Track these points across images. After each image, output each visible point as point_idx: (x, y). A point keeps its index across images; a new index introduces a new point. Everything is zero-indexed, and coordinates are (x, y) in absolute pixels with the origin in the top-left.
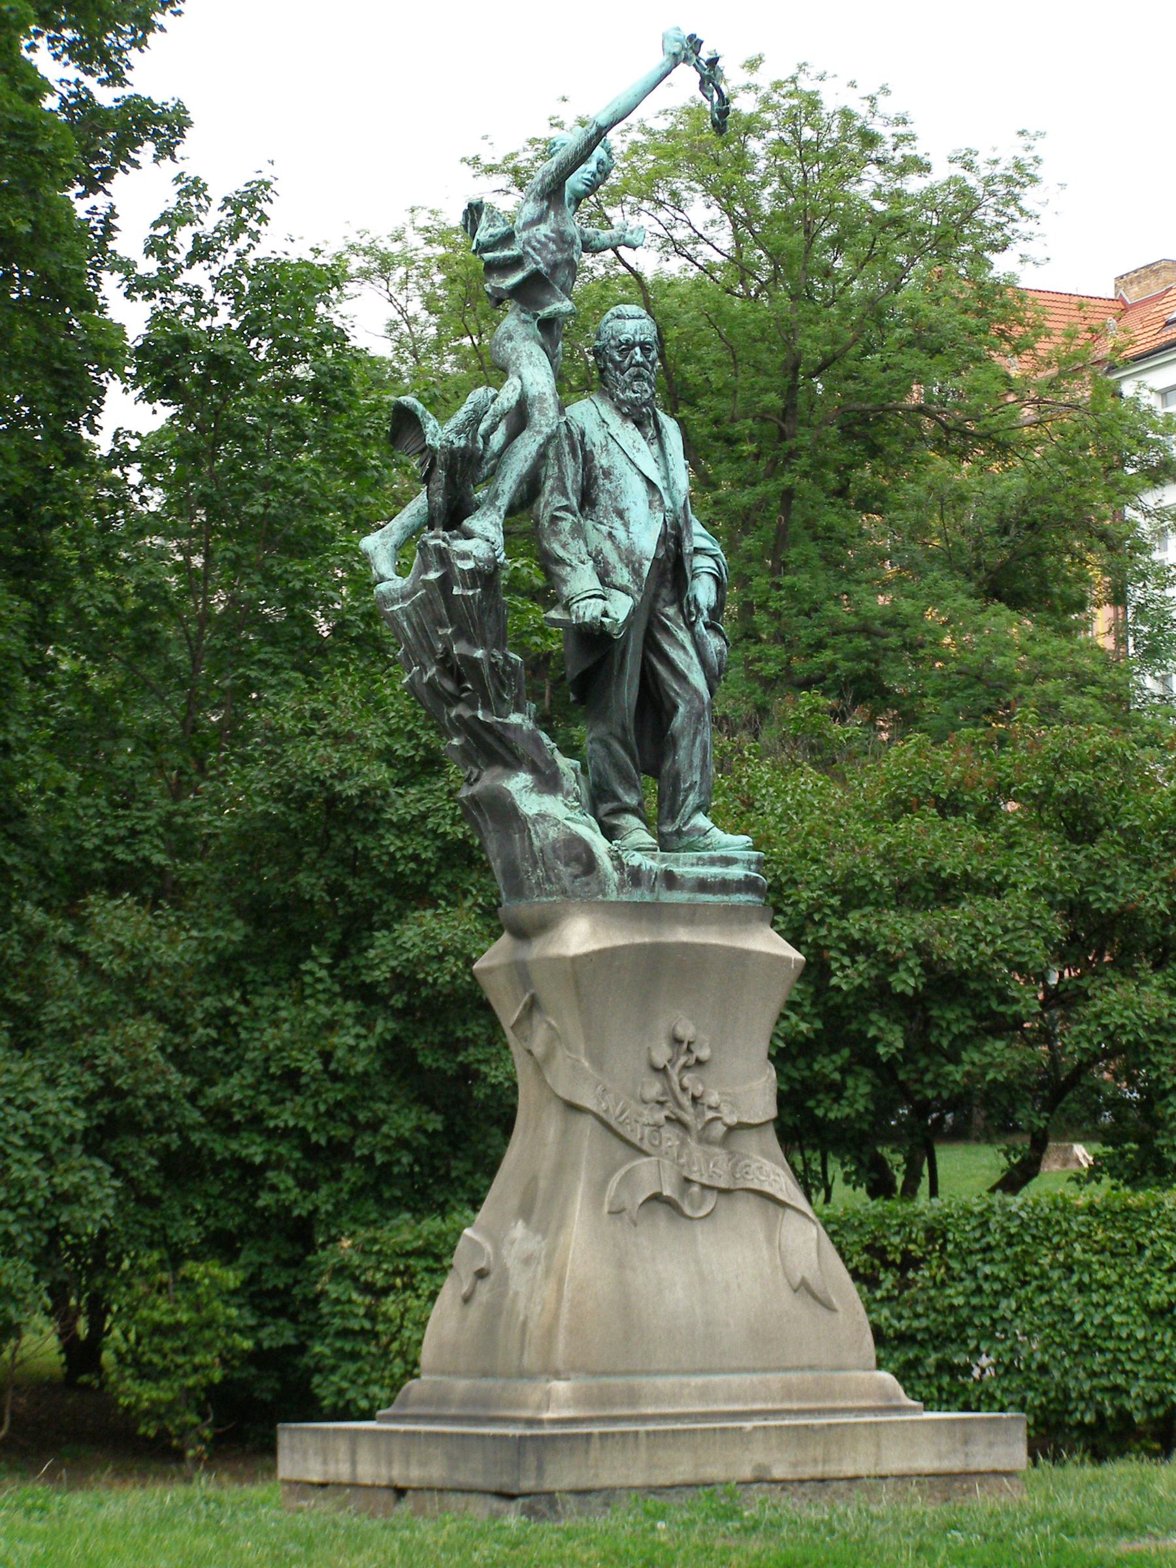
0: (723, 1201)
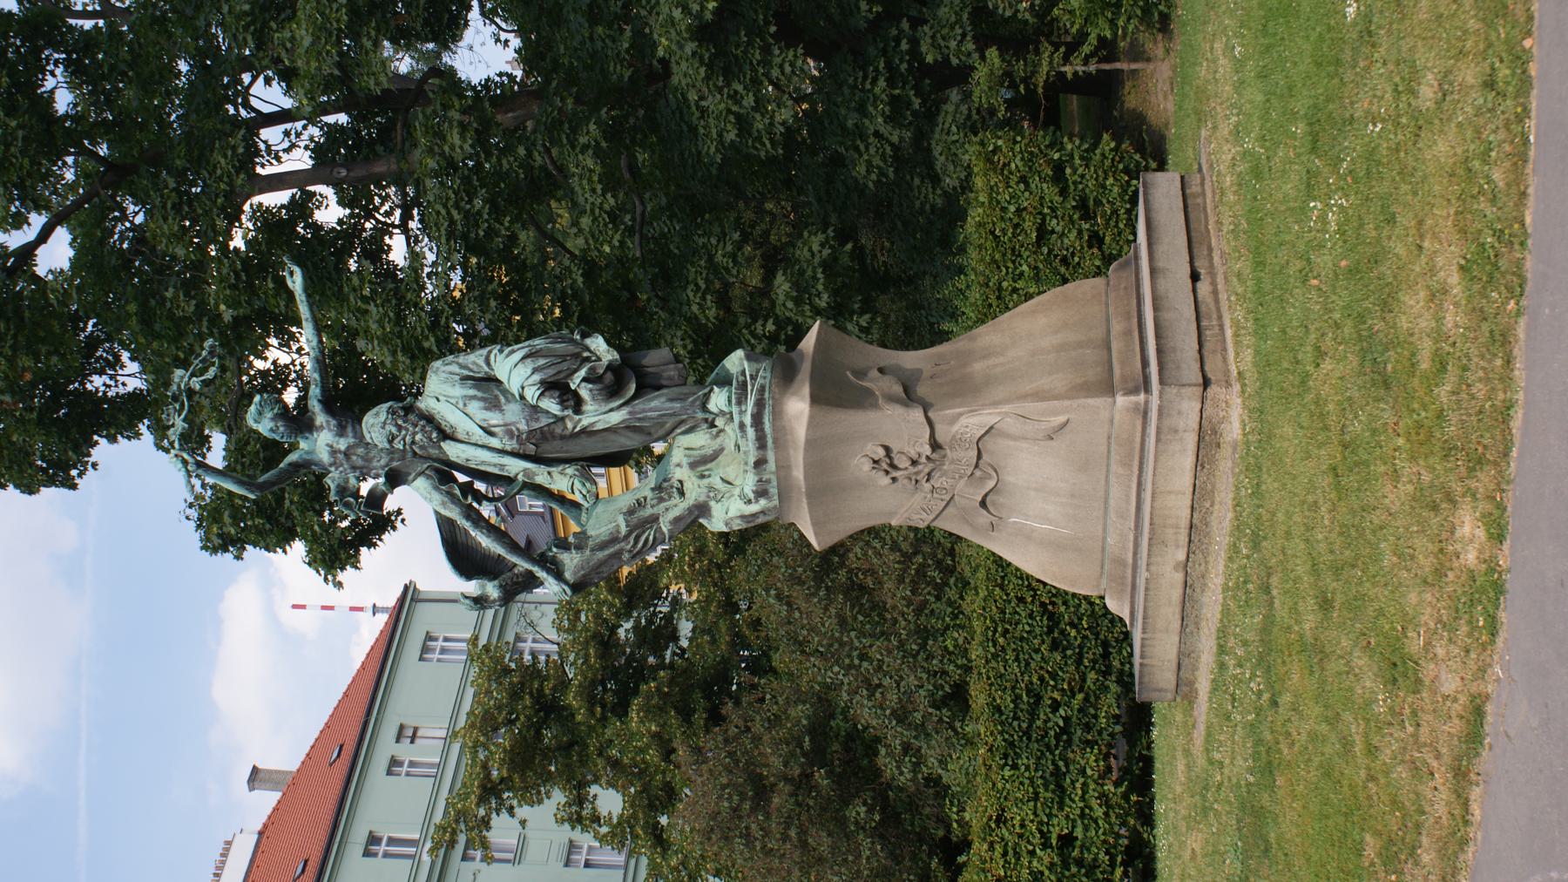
0: (985, 457)
